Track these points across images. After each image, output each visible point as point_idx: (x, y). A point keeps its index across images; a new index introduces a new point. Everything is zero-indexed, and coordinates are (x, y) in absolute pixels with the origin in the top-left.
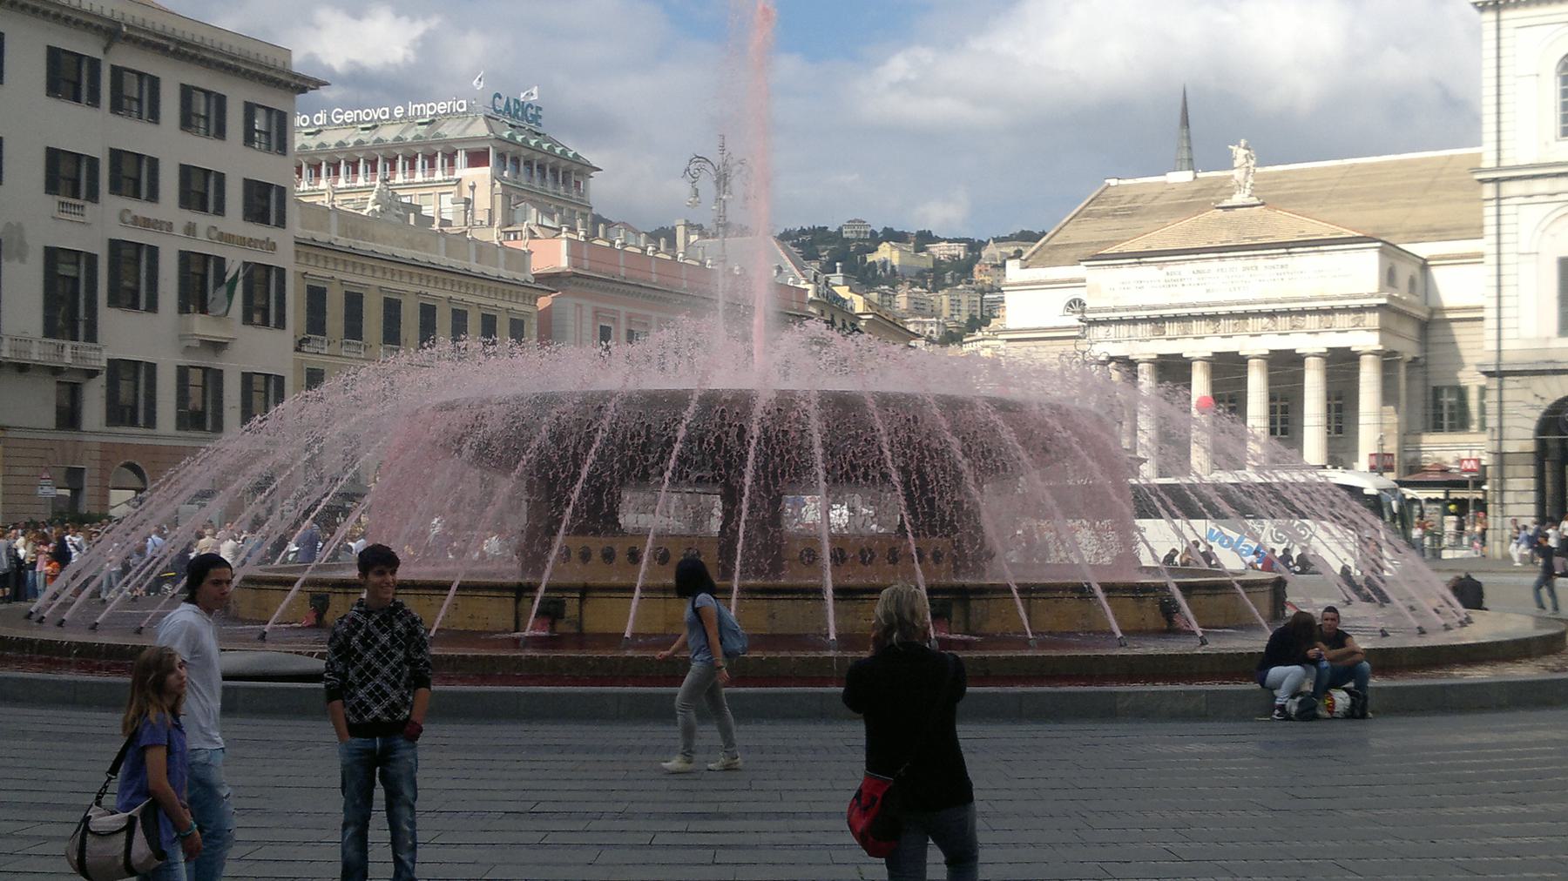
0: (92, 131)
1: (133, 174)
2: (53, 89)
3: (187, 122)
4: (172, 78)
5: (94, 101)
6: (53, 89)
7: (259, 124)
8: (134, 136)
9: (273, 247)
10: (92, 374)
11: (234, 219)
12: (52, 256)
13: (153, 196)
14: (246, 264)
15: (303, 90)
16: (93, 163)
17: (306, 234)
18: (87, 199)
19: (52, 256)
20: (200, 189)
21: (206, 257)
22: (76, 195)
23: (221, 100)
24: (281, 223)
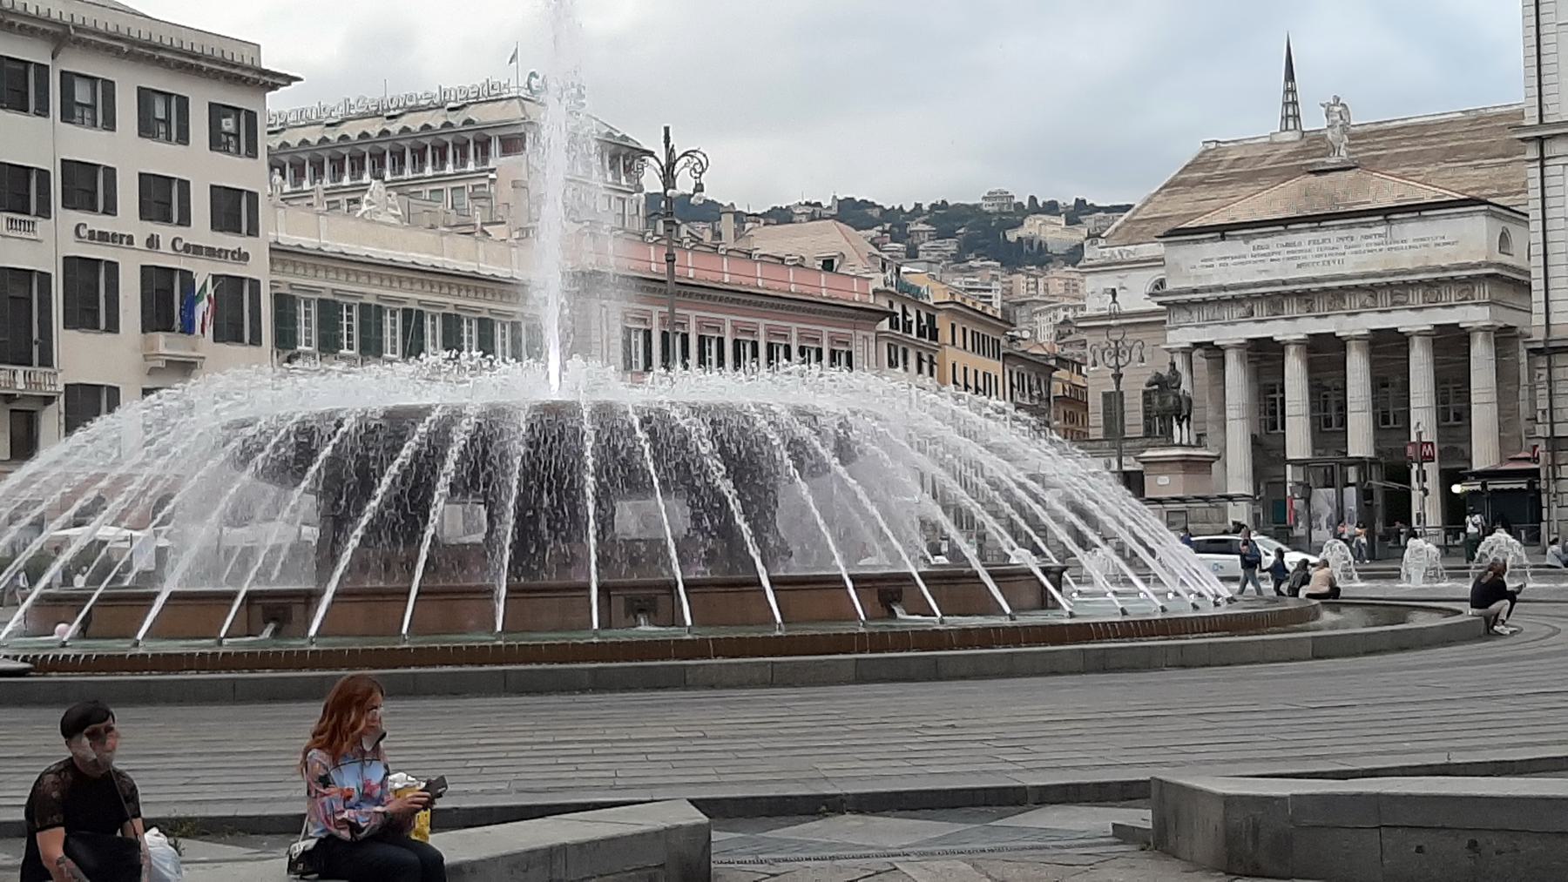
1: (86, 185)
4: (128, 83)
5: (43, 110)
8: (86, 144)
9: (246, 257)
10: (48, 400)
11: (200, 230)
13: (110, 209)
14: (215, 278)
15: (274, 87)
16: (44, 175)
17: (288, 239)
18: (37, 215)
20: (161, 198)
23: (183, 102)
24: (253, 231)
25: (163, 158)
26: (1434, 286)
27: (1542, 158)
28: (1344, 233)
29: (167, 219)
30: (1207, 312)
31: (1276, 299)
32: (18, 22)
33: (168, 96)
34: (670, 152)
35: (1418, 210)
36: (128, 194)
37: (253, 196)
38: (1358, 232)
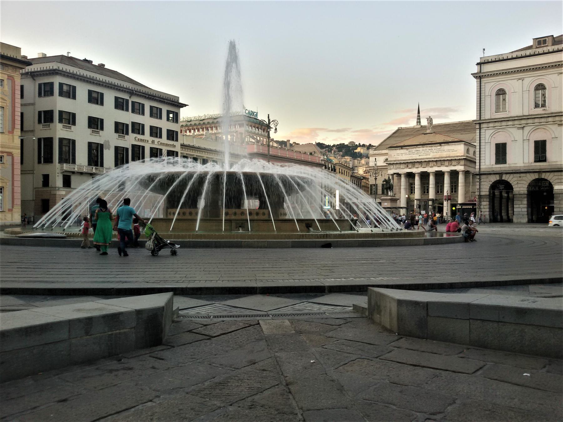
0: (127, 117)
1: (138, 128)
2: (117, 107)
3: (151, 115)
6: (117, 107)
7: (171, 115)
8: (138, 118)
9: (175, 146)
12: (117, 148)
15: (182, 107)
16: (127, 125)
19: (117, 148)
20: (155, 132)
21: (157, 149)
22: (123, 134)
24: (177, 140)
25: (156, 122)
26: (450, 161)
27: (480, 128)
28: (430, 148)
29: (157, 137)
30: (398, 166)
31: (413, 163)
32: (121, 89)
33: (157, 108)
34: (269, 120)
35: (447, 143)
36: (147, 130)
37: (177, 132)
38: (433, 148)
